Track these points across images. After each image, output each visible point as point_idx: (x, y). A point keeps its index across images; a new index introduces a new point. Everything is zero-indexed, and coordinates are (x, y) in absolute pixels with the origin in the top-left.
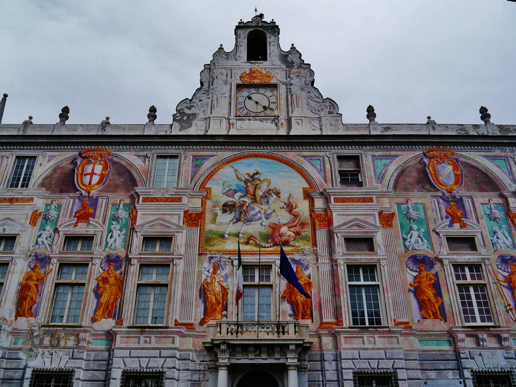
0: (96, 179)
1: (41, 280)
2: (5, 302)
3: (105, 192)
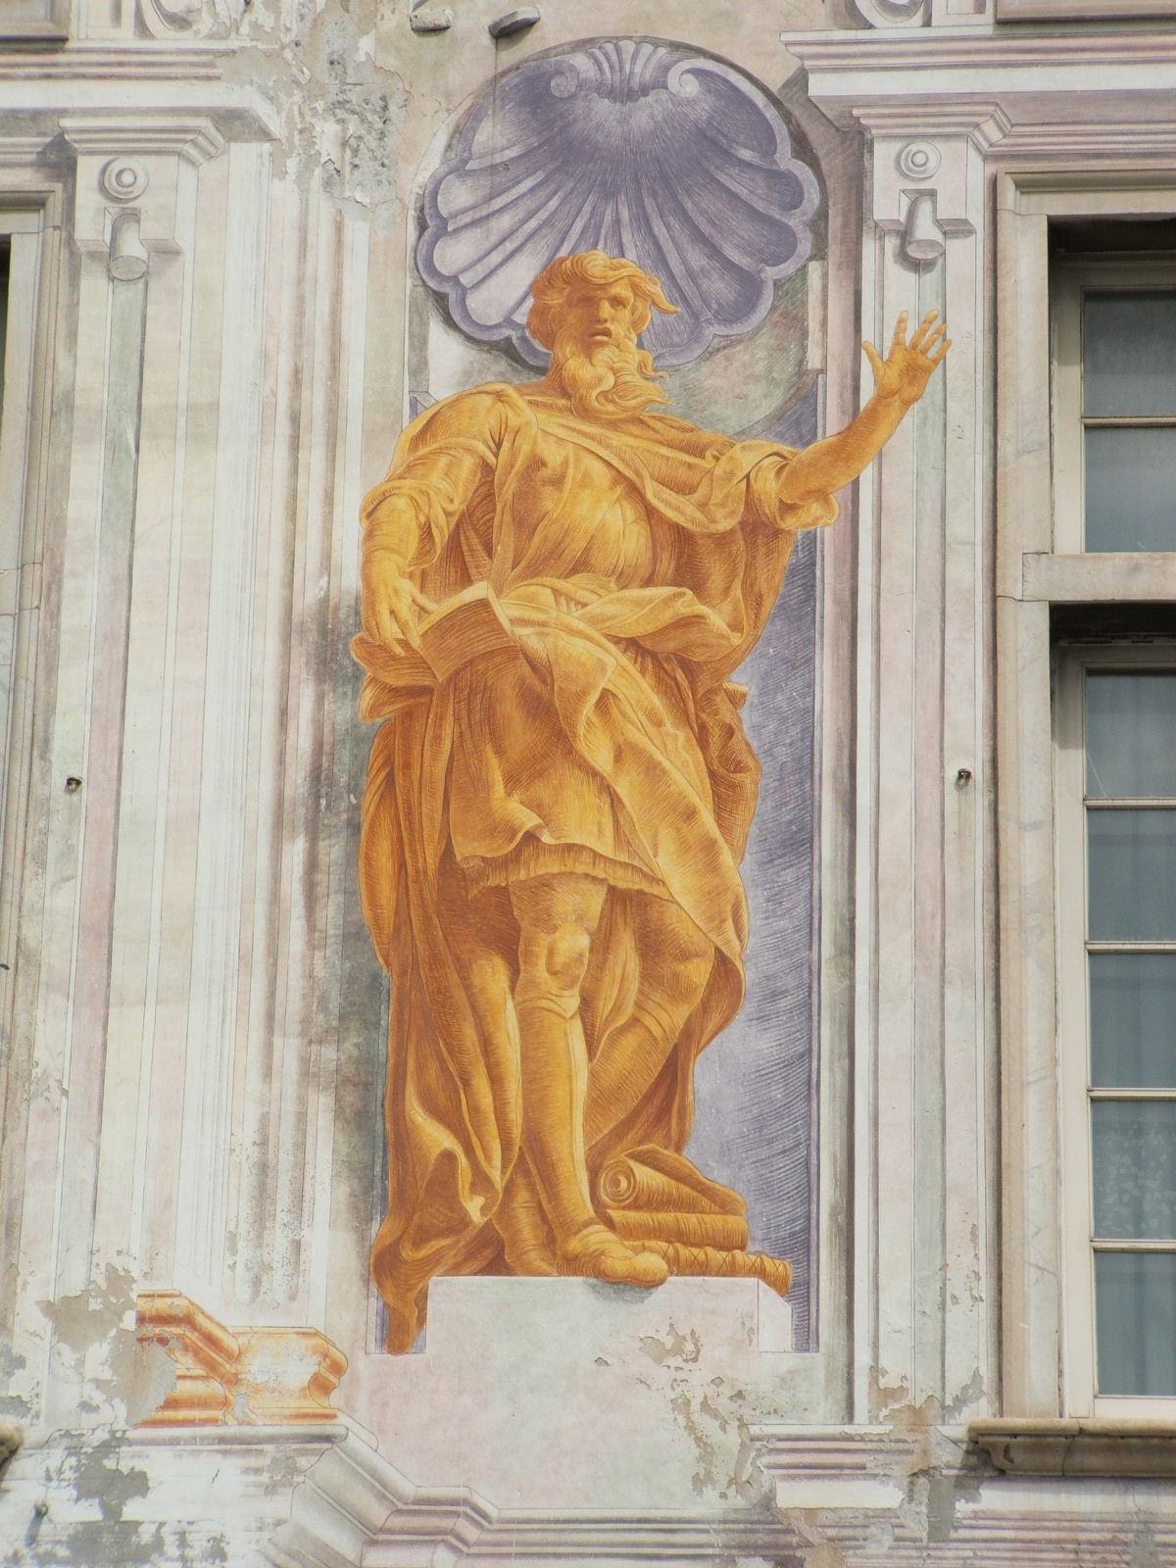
1: (752, 568)
2: (101, 1001)
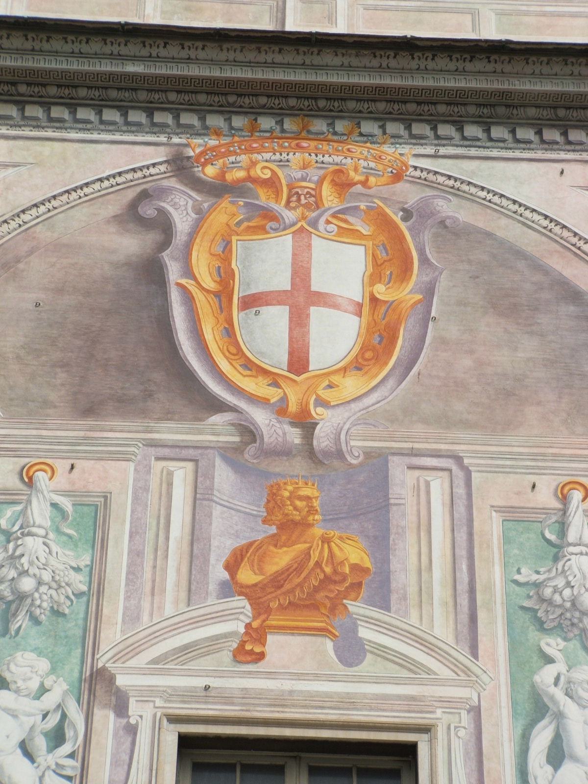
0: (335, 336)
3: (425, 421)
